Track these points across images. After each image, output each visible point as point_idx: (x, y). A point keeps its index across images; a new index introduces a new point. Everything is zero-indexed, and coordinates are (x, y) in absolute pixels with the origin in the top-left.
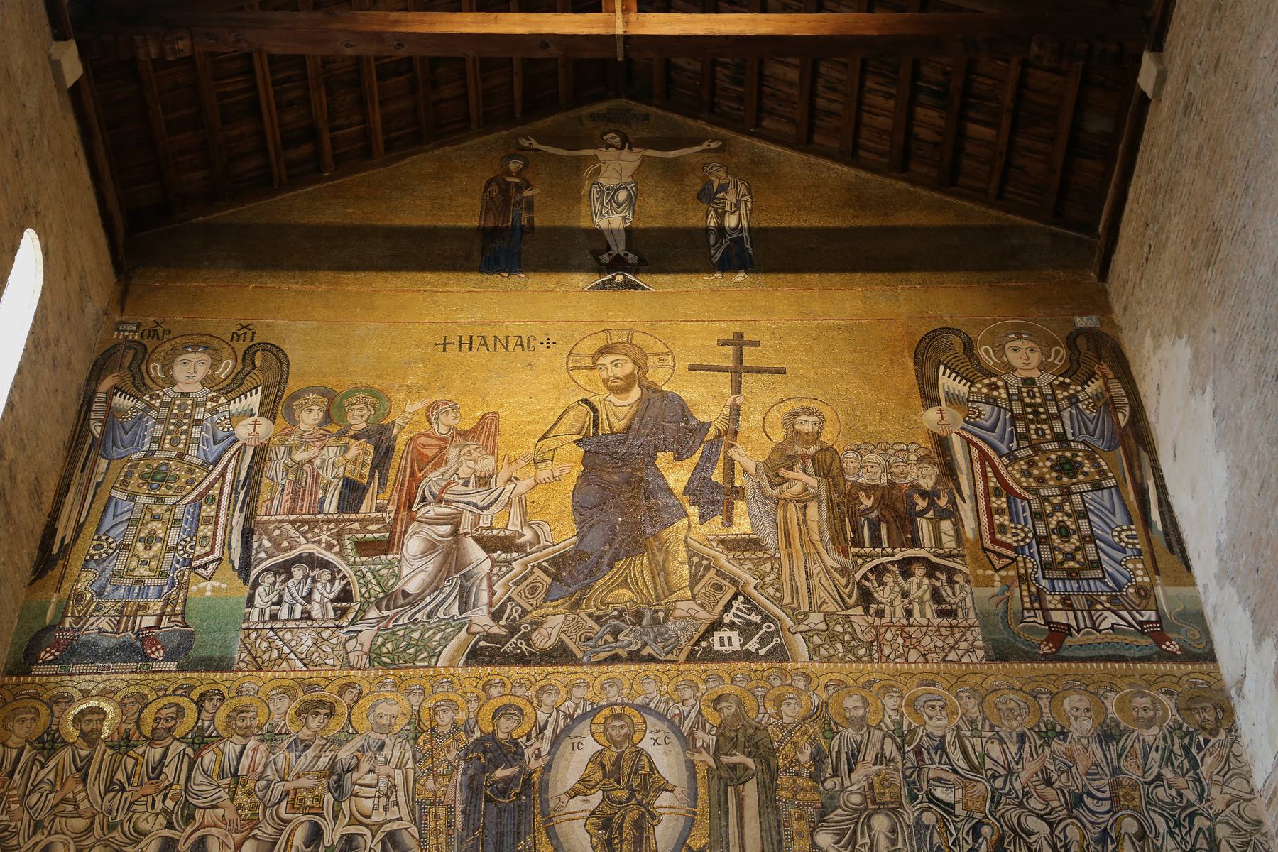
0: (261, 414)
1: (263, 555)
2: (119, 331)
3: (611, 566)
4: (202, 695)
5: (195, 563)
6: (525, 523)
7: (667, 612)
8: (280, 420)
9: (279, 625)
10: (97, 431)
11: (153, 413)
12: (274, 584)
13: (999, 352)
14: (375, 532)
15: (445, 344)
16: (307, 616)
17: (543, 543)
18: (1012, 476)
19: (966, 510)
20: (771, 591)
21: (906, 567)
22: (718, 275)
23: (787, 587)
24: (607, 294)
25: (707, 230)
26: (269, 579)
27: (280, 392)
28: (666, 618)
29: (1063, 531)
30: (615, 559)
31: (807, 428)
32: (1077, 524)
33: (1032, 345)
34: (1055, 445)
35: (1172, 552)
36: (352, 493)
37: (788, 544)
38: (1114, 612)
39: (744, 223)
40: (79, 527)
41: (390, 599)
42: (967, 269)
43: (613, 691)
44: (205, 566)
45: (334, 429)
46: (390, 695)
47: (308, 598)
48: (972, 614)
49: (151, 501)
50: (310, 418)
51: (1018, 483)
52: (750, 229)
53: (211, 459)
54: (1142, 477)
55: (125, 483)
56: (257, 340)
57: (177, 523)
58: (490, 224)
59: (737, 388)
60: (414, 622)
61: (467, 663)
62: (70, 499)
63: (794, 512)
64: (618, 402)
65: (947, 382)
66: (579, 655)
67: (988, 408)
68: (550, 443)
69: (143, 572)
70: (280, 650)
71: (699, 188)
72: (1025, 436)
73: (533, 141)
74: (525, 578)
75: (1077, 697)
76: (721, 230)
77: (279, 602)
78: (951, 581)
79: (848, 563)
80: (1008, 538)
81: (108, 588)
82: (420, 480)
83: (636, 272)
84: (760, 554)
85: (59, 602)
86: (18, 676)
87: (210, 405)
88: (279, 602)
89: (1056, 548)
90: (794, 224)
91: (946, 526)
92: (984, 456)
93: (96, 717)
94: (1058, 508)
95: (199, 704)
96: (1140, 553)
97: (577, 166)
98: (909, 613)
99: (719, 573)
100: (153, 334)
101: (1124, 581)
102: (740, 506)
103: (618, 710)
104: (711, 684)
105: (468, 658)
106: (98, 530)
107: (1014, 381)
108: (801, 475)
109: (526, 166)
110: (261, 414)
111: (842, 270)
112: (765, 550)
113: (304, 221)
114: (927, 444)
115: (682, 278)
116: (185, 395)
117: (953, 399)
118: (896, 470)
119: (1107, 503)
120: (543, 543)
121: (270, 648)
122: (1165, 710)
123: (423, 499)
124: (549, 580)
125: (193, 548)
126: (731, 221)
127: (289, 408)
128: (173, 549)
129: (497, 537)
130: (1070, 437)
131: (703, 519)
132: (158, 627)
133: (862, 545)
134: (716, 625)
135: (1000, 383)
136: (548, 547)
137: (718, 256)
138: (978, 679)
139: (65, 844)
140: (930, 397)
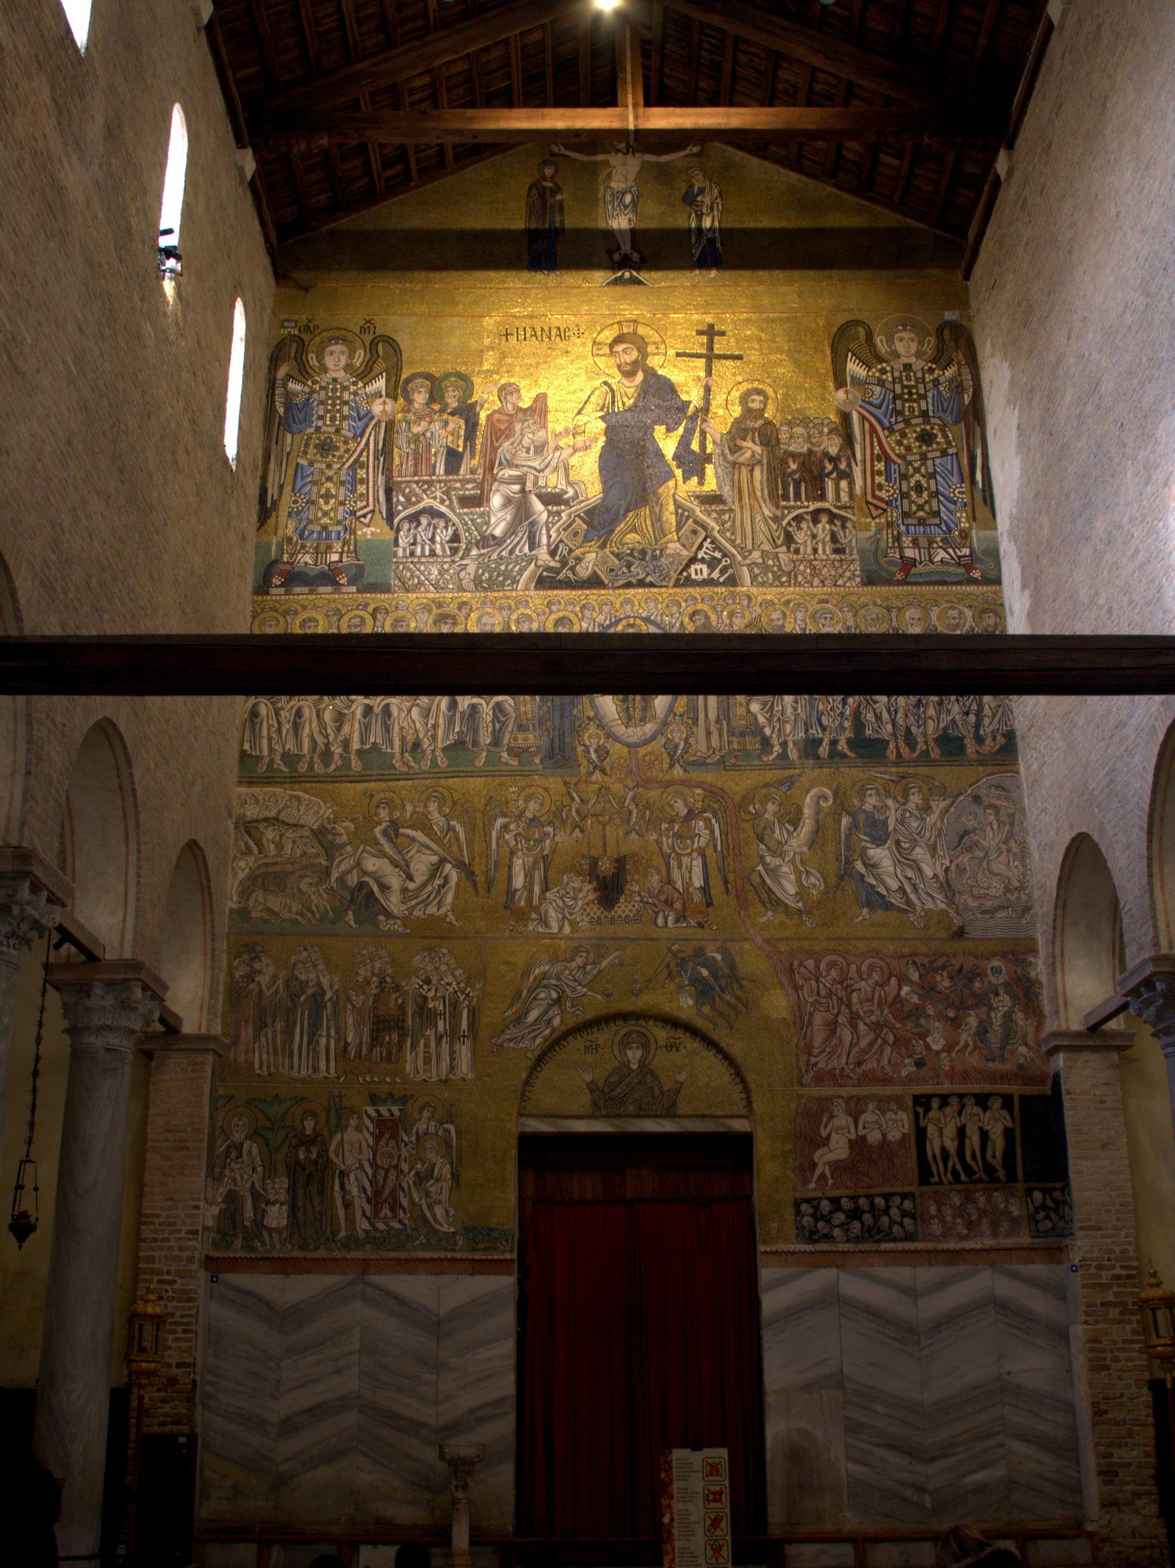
0: (387, 396)
1: (400, 508)
2: (283, 327)
3: (625, 516)
4: (374, 610)
5: (358, 514)
6: (569, 483)
7: (661, 551)
8: (401, 400)
9: (416, 560)
10: (281, 410)
11: (315, 396)
12: (409, 530)
13: (890, 341)
14: (471, 490)
15: (507, 335)
16: (433, 553)
17: (581, 498)
18: (890, 445)
19: (857, 472)
20: (728, 534)
21: (815, 516)
22: (697, 272)
23: (739, 531)
24: (619, 290)
25: (689, 230)
26: (406, 526)
27: (399, 376)
28: (661, 555)
29: (919, 488)
30: (628, 511)
31: (756, 404)
32: (928, 483)
33: (913, 335)
34: (919, 420)
35: (985, 503)
36: (453, 459)
37: (741, 499)
38: (945, 550)
39: (716, 224)
40: (281, 487)
41: (487, 541)
43: (628, 608)
44: (364, 516)
45: (436, 407)
46: (490, 610)
47: (433, 540)
48: (855, 552)
49: (324, 466)
50: (420, 398)
51: (893, 450)
52: (720, 229)
53: (358, 432)
54: (974, 446)
55: (305, 453)
56: (378, 333)
57: (342, 483)
58: (533, 226)
59: (709, 372)
60: (501, 558)
61: (536, 588)
62: (272, 466)
63: (744, 470)
64: (628, 384)
65: (854, 368)
66: (606, 582)
67: (877, 389)
68: (582, 419)
69: (326, 520)
70: (418, 578)
71: (684, 191)
72: (900, 413)
73: (562, 148)
74: (570, 525)
75: (913, 610)
76: (700, 231)
77: (414, 544)
78: (844, 527)
79: (779, 513)
80: (883, 494)
81: (306, 533)
82: (497, 449)
84: (722, 507)
85: (278, 543)
86: (262, 595)
87: (353, 388)
88: (414, 544)
89: (913, 502)
90: (752, 225)
91: (844, 484)
92: (873, 429)
93: (312, 624)
94: (917, 470)
95: (374, 616)
96: (965, 505)
97: (593, 171)
98: (815, 551)
99: (696, 522)
100: (307, 329)
101: (952, 526)
102: (710, 469)
103: (631, 621)
104: (690, 603)
105: (537, 583)
106: (293, 489)
107: (898, 366)
108: (750, 444)
109: (557, 171)
110: (387, 396)
111: (785, 266)
112: (723, 502)
114: (833, 417)
115: (672, 274)
116: (335, 380)
117: (856, 381)
118: (813, 440)
119: (949, 467)
120: (581, 498)
121: (412, 577)
122: (966, 619)
123: (501, 464)
124: (585, 527)
125: (355, 502)
126: (707, 223)
127: (405, 389)
128: (342, 503)
129: (551, 494)
130: (931, 414)
131: (686, 479)
132: (341, 561)
133: (788, 500)
134: (693, 560)
135: (888, 368)
136: (582, 501)
137: (697, 255)
138: (854, 598)
139: (309, 707)
140: (840, 383)
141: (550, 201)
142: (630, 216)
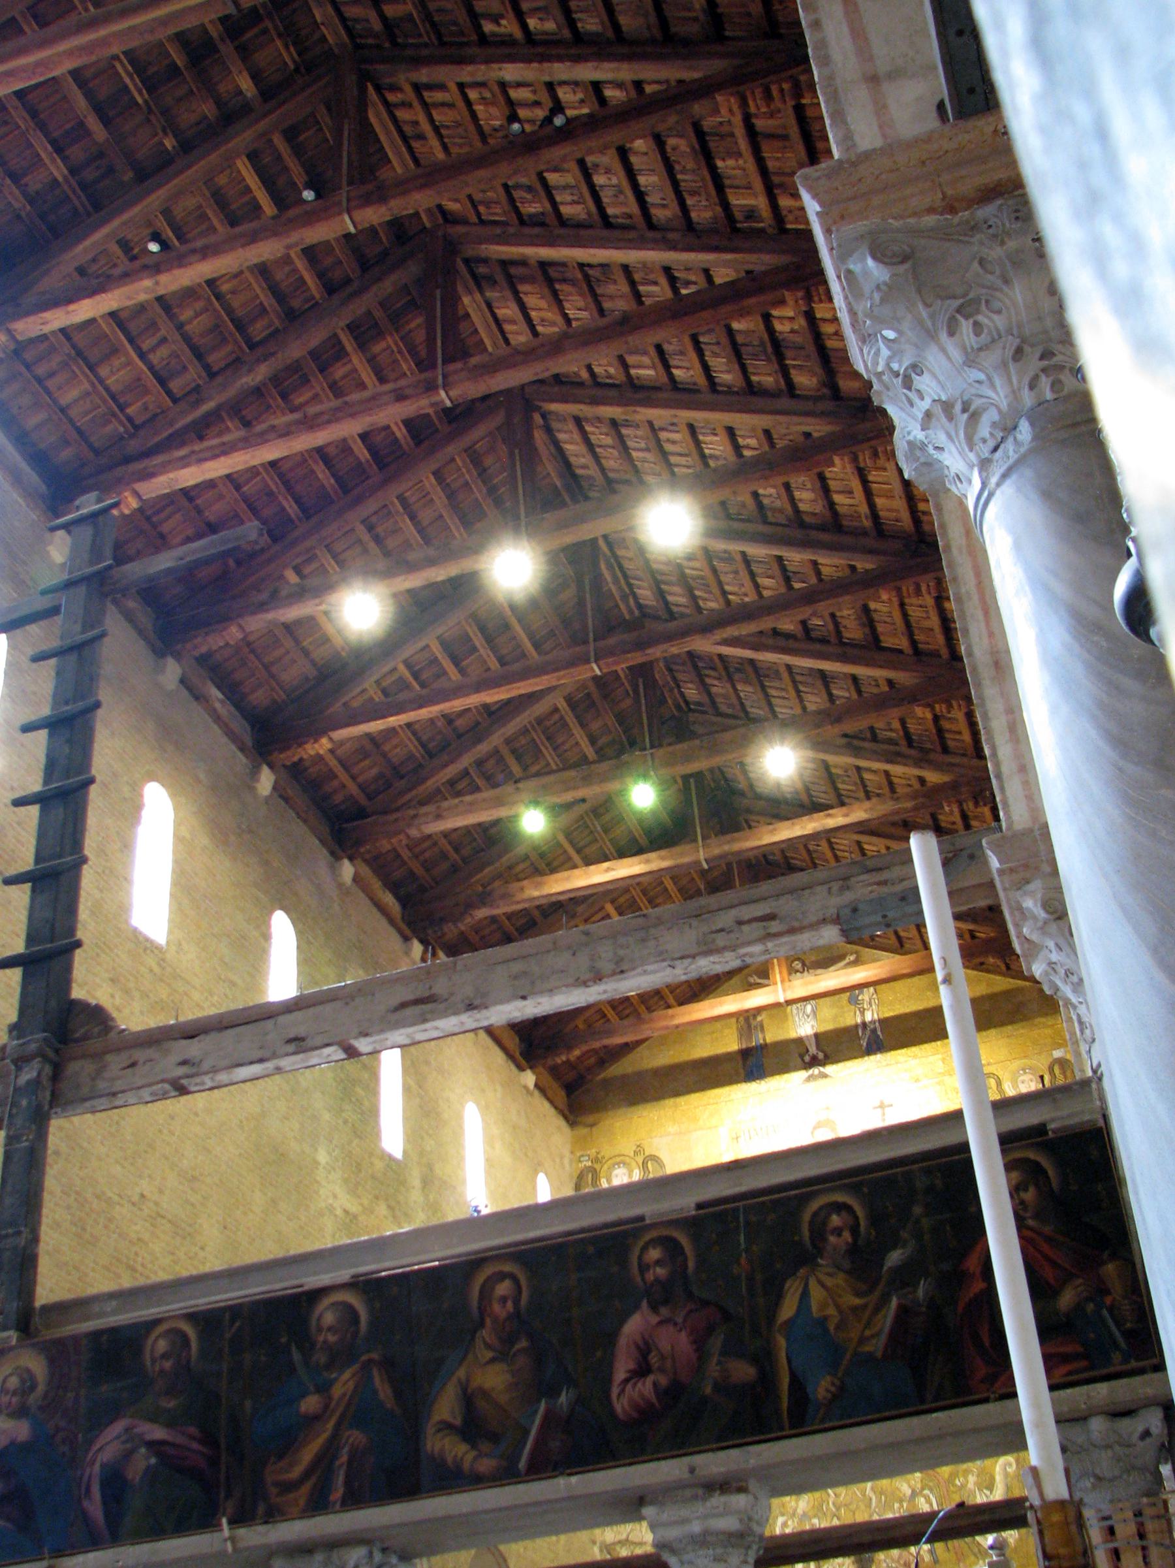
24: (813, 1084)
25: (857, 1026)
42: (995, 1027)
58: (744, 1046)
76: (864, 1024)
83: (823, 1064)
100: (596, 1160)
113: (650, 1066)
126: (868, 1017)
141: (753, 1023)
142: (813, 1023)
